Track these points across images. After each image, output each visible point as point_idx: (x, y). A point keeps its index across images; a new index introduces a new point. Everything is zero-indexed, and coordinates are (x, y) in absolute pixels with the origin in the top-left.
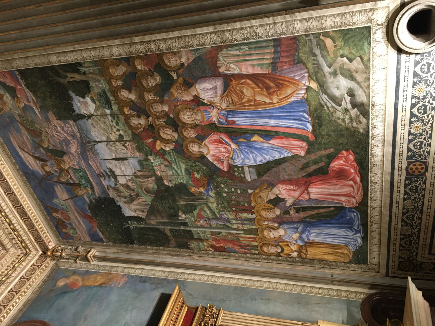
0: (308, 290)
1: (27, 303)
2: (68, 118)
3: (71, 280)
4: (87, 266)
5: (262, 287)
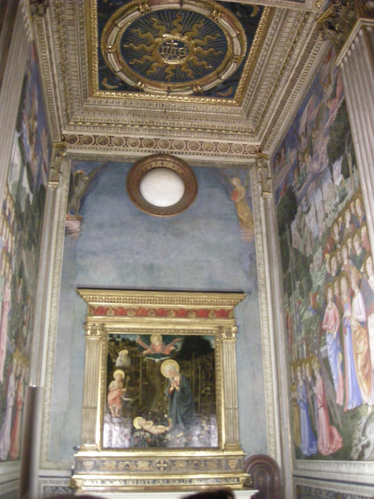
0: (271, 409)
1: (212, 163)
2: (329, 157)
3: (240, 189)
4: (256, 196)
5: (266, 368)
